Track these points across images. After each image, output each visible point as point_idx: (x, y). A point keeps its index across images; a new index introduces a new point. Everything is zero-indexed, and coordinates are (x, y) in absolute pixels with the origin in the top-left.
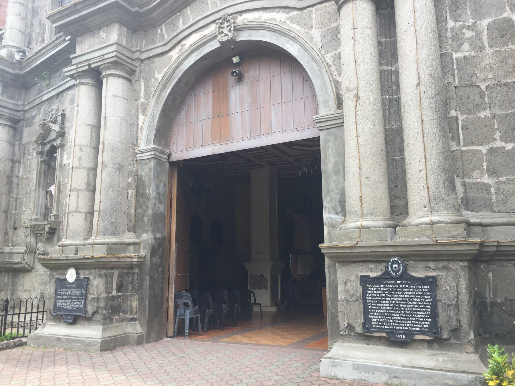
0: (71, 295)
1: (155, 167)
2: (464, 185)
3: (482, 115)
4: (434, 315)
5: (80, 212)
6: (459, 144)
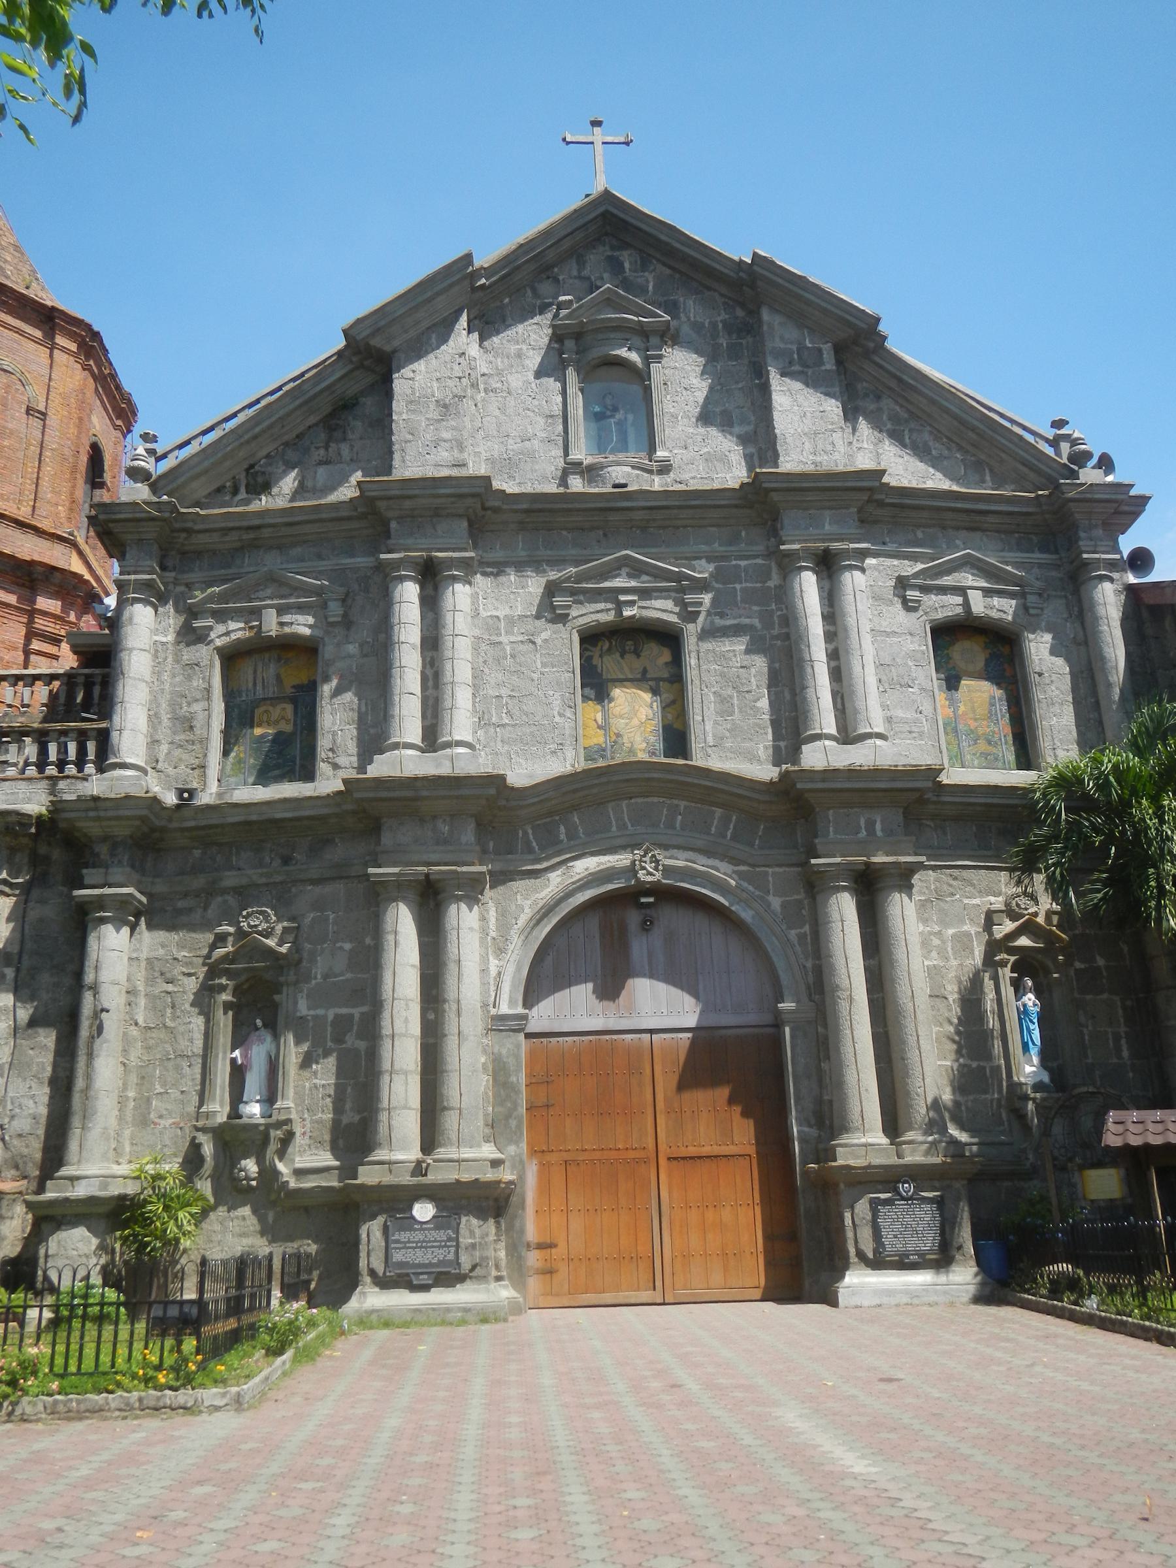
0: (424, 1241)
5: (410, 1109)
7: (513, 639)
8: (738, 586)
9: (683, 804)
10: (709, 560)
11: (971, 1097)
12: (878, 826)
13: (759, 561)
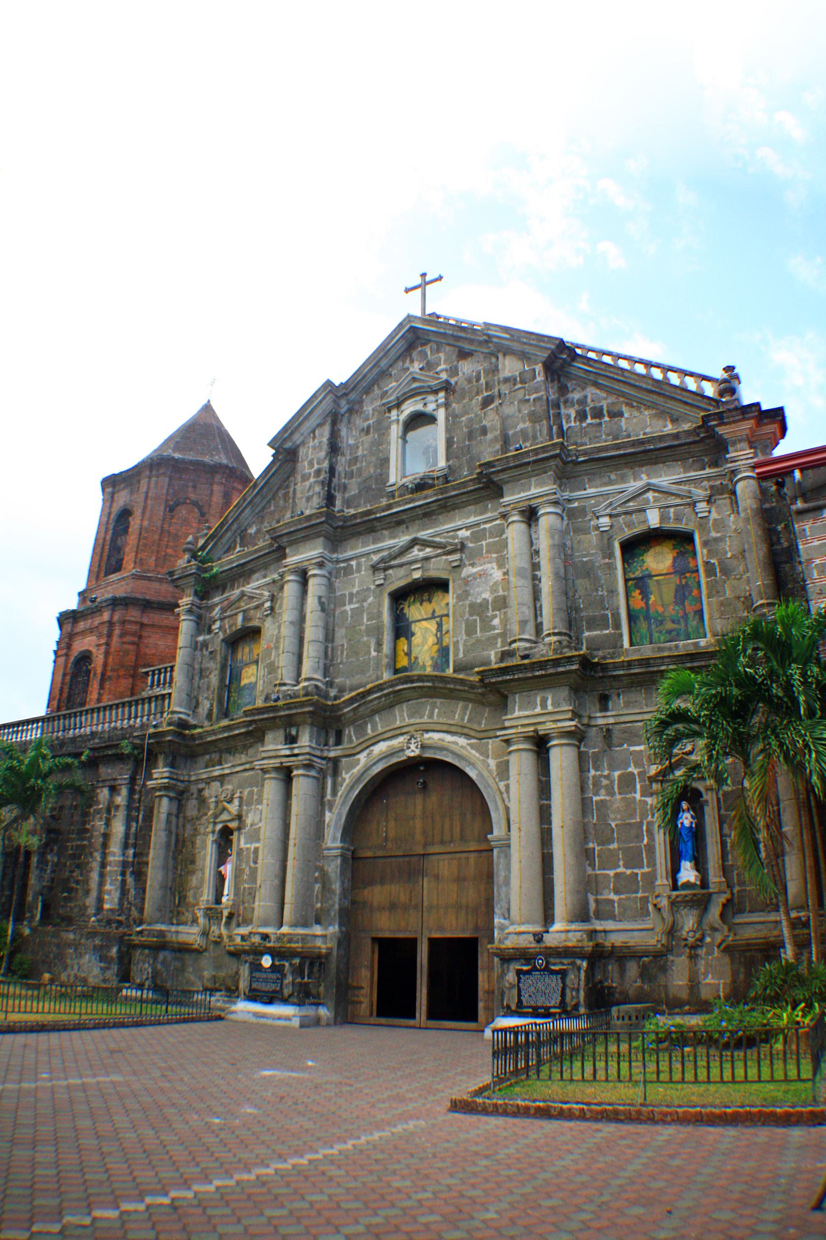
1: (342, 865)
2: (597, 901)
3: (611, 847)
4: (563, 994)
6: (594, 869)
7: (352, 606)
8: (484, 543)
9: (438, 701)
10: (467, 528)
11: (623, 896)
12: (549, 702)
13: (498, 522)
